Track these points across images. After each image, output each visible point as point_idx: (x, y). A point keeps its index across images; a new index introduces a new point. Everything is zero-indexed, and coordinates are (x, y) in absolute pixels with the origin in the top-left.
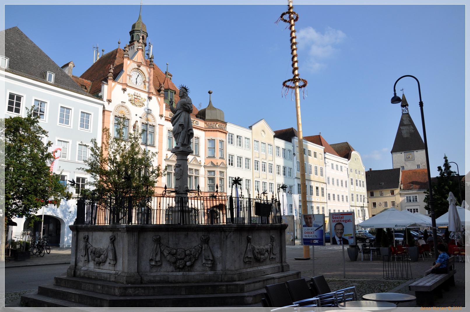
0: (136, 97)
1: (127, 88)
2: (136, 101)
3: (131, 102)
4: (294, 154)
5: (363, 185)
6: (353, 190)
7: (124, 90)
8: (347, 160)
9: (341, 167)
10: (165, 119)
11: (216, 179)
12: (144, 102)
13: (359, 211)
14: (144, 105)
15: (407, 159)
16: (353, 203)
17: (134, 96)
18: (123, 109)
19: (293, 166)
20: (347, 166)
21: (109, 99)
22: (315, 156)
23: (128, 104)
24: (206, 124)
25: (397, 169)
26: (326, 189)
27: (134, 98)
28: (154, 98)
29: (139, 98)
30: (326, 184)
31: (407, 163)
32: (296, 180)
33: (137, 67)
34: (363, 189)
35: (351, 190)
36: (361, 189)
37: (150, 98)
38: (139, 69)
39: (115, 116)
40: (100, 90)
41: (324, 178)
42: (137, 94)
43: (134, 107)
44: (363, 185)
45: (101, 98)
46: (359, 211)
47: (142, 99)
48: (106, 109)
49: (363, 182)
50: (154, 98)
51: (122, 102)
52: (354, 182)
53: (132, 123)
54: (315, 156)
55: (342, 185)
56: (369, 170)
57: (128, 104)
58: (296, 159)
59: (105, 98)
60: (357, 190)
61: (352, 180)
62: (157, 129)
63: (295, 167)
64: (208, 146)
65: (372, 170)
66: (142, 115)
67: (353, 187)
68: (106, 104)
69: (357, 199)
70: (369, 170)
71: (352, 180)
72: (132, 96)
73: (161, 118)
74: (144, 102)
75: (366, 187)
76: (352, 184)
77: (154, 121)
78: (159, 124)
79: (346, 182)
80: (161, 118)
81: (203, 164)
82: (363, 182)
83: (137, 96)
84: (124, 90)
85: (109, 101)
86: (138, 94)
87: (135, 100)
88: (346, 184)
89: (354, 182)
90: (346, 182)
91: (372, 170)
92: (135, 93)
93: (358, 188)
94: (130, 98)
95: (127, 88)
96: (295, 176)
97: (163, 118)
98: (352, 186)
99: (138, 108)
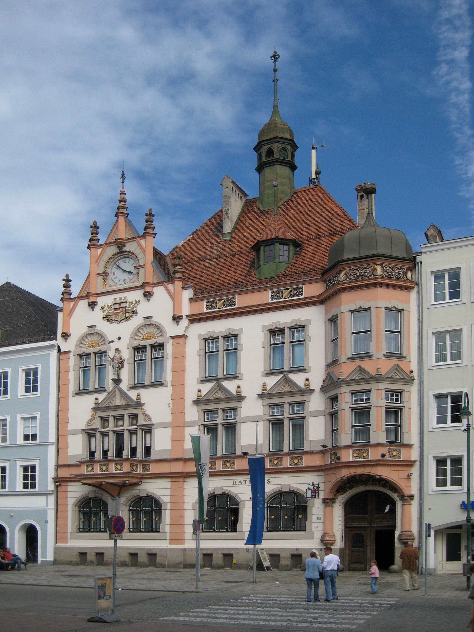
0: (117, 306)
3: (108, 320)
7: (92, 305)
11: (373, 412)
14: (136, 314)
27: (113, 311)
29: (123, 305)
37: (148, 295)
42: (120, 299)
43: (115, 326)
47: (131, 303)
62: (169, 349)
72: (110, 307)
74: (136, 307)
77: (162, 335)
83: (120, 304)
87: (115, 312)
92: (115, 299)
94: (105, 313)
97: (185, 322)
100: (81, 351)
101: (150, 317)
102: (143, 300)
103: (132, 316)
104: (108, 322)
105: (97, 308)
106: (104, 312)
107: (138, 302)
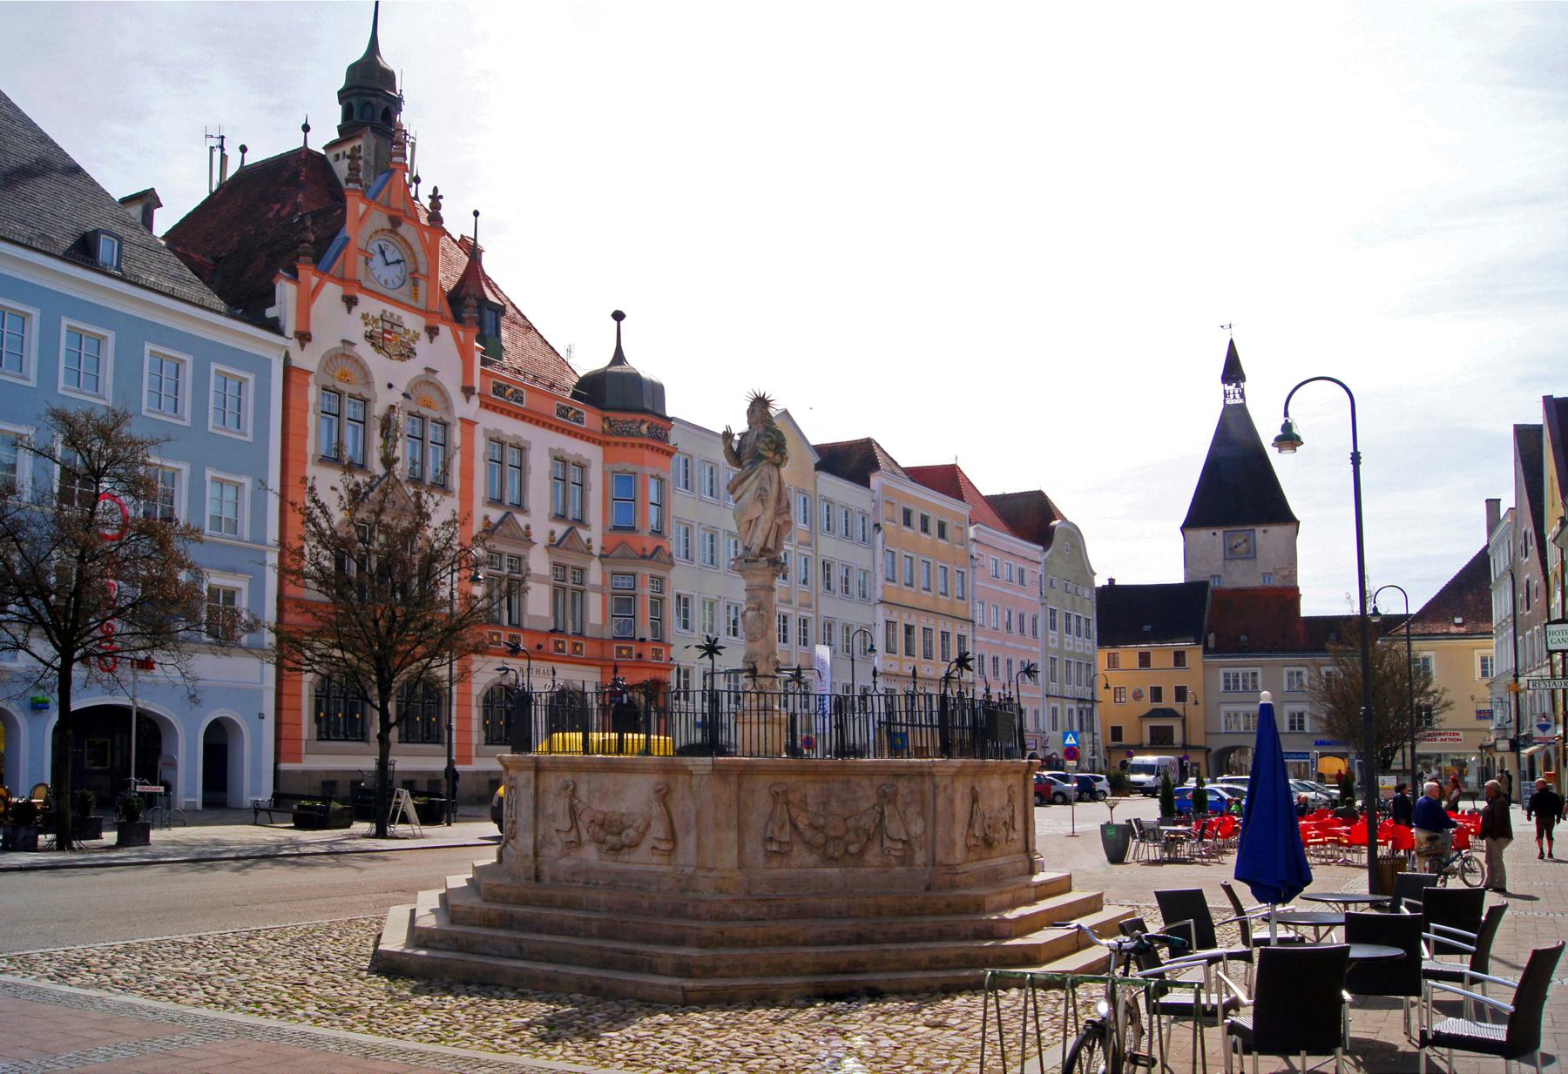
0: (388, 326)
1: (361, 297)
2: (390, 340)
3: (373, 345)
4: (877, 526)
5: (1088, 631)
6: (1056, 645)
7: (350, 302)
8: (1041, 548)
9: (1021, 571)
10: (481, 402)
12: (414, 342)
13: (1071, 711)
15: (1231, 553)
16: (1054, 688)
17: (380, 322)
18: (348, 366)
19: (874, 563)
20: (1040, 570)
21: (302, 329)
22: (942, 535)
23: (365, 351)
24: (606, 422)
25: (1199, 583)
26: (974, 641)
27: (380, 330)
28: (445, 331)
30: (974, 626)
31: (1232, 566)
32: (880, 609)
33: (388, 225)
34: (1086, 645)
35: (1050, 644)
36: (1081, 644)
37: (432, 332)
38: (397, 234)
39: (323, 389)
40: (269, 298)
41: (967, 605)
42: (392, 315)
44: (1088, 631)
45: (274, 326)
46: (1071, 711)
48: (294, 364)
49: (1088, 621)
50: (445, 331)
51: (344, 341)
52: (1060, 620)
53: (378, 409)
54: (942, 535)
55: (1022, 630)
56: (1107, 583)
57: (365, 351)
58: (883, 543)
59: (290, 327)
60: (1069, 645)
61: (1053, 612)
63: (878, 569)
64: (612, 494)
65: (1117, 583)
66: (407, 388)
67: (1057, 638)
68: (293, 345)
69: (1068, 672)
70: (1107, 583)
71: (1053, 612)
72: (376, 321)
73: (468, 399)
74: (414, 342)
75: (1096, 637)
76: (1053, 627)
78: (461, 419)
79: (1035, 619)
80: (468, 399)
81: (596, 550)
82: (1088, 621)
83: (393, 324)
84: (350, 302)
85: (304, 337)
86: (395, 317)
88: (1034, 626)
89: (1060, 620)
90: (1035, 619)
91: (1117, 583)
92: (385, 311)
93: (1071, 642)
94: (369, 328)
95: (361, 297)
96: (879, 594)
97: (475, 400)
98: (1052, 635)
99: (396, 364)
100: (329, 382)
101: (435, 372)
102: (424, 336)
103: (409, 357)
104: (372, 348)
105: (358, 311)
106: (366, 324)
107: (417, 336)
